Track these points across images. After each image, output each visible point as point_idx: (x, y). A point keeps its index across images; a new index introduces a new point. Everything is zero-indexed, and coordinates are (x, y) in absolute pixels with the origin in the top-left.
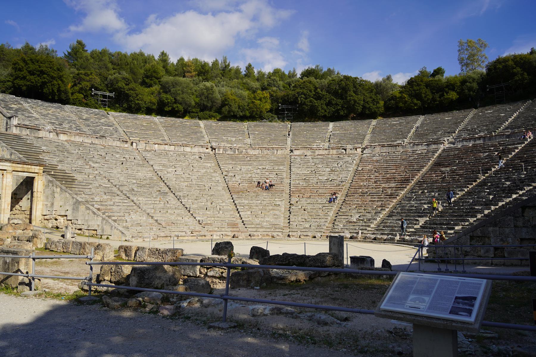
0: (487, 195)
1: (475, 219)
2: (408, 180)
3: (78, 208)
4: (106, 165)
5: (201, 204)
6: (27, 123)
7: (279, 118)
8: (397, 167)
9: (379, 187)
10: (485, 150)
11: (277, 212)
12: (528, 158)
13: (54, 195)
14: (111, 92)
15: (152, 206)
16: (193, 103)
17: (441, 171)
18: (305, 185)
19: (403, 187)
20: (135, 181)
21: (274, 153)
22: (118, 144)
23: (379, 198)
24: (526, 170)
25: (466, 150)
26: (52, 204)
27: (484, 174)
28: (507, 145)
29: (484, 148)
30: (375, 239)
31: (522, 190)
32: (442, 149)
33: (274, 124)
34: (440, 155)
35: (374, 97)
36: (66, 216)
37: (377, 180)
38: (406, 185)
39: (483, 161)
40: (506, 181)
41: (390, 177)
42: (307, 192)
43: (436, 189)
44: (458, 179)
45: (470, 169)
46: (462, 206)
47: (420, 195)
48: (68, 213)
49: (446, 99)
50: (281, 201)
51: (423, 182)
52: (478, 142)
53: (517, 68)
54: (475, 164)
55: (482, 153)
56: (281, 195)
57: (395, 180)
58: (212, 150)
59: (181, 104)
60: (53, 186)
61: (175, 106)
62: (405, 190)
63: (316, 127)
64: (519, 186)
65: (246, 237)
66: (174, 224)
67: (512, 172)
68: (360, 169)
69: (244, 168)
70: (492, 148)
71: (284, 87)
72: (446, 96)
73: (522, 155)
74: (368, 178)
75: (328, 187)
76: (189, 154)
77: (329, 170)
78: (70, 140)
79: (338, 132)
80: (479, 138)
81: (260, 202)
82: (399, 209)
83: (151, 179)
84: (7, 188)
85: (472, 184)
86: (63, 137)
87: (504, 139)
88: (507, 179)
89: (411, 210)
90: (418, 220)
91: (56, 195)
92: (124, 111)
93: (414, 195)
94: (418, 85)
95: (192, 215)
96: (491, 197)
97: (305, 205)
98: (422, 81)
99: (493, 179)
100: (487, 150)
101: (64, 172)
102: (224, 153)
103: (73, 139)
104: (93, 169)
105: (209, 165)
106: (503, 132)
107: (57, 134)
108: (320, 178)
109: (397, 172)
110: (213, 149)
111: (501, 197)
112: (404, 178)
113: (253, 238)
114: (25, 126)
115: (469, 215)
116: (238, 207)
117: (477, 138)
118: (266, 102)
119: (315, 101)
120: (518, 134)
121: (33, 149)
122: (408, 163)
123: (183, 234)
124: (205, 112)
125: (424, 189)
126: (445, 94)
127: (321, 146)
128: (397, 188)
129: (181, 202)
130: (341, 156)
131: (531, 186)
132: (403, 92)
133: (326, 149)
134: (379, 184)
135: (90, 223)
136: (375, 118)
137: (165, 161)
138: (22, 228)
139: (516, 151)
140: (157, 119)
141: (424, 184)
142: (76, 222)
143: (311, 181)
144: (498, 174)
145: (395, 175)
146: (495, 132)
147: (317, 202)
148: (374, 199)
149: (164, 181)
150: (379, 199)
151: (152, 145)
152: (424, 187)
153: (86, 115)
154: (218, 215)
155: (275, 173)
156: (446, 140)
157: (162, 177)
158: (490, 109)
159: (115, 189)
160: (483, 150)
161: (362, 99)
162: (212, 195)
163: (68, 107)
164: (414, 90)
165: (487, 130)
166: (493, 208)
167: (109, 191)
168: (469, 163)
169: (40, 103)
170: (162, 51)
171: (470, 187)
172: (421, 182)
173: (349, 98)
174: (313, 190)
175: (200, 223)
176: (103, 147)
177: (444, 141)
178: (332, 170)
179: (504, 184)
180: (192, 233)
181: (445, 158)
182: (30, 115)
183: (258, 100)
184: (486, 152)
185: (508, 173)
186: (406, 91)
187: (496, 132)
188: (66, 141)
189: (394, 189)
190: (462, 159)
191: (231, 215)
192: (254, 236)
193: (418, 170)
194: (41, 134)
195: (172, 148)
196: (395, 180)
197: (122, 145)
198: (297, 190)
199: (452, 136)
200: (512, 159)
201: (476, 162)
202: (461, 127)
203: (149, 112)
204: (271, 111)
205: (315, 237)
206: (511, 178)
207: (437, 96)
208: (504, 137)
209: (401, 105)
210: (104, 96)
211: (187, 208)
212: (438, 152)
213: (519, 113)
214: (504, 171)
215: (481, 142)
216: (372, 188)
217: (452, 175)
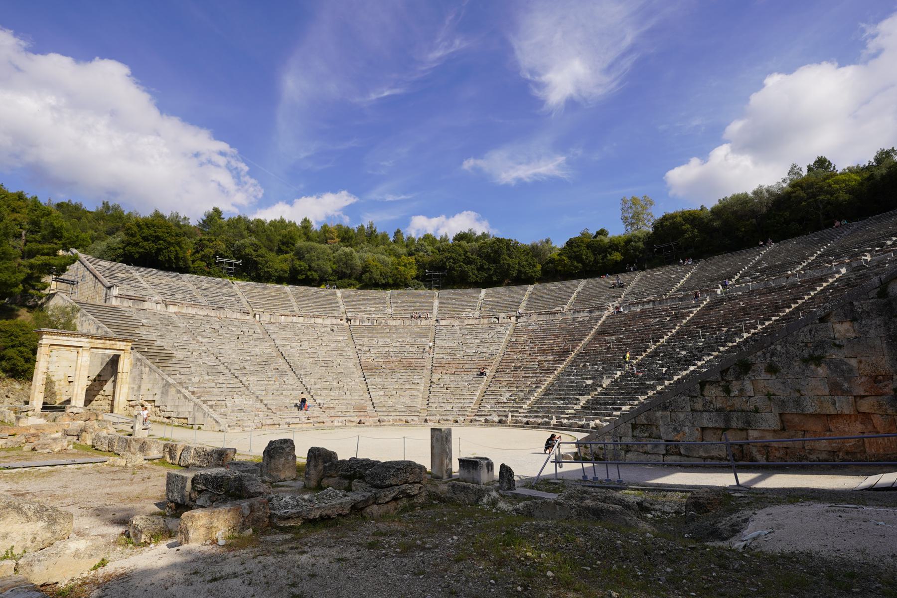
0: (659, 367)
1: (646, 397)
3: (167, 391)
4: (217, 340)
5: (325, 383)
6: (131, 293)
7: (426, 286)
8: (556, 336)
11: (414, 392)
12: (705, 323)
13: (141, 376)
14: (238, 259)
15: (263, 388)
16: (330, 270)
17: (605, 341)
18: (450, 359)
20: (249, 358)
22: (238, 316)
23: (533, 373)
24: (704, 336)
25: (634, 317)
26: (139, 387)
27: (655, 342)
28: (680, 309)
29: (654, 314)
30: (527, 423)
31: (700, 361)
33: (420, 291)
34: (604, 322)
35: (530, 260)
36: (154, 401)
39: (653, 328)
40: (680, 350)
43: (600, 361)
44: (625, 350)
45: (639, 337)
46: (631, 381)
48: (157, 398)
49: (609, 260)
50: (421, 378)
51: (585, 353)
52: (647, 306)
53: (686, 224)
56: (421, 371)
58: (347, 322)
59: (316, 271)
60: (141, 365)
61: (309, 273)
62: (565, 363)
63: (466, 294)
64: (696, 355)
65: (374, 423)
66: (287, 408)
67: (688, 340)
68: (513, 339)
69: (381, 341)
70: (663, 313)
72: (609, 257)
73: (698, 320)
75: (476, 362)
76: (320, 326)
77: (479, 341)
78: (180, 312)
79: (491, 299)
80: (648, 302)
81: (395, 380)
82: (557, 385)
83: (270, 355)
84: (82, 369)
85: (641, 355)
86: (172, 309)
87: (677, 303)
88: (683, 348)
89: (571, 387)
90: (578, 399)
91: (144, 376)
92: (252, 279)
93: (575, 369)
94: (578, 246)
95: (312, 396)
96: (664, 369)
98: (582, 242)
99: (667, 349)
101: (162, 348)
102: (361, 324)
103: (184, 310)
104: (200, 344)
105: (341, 338)
107: (166, 306)
108: (468, 351)
110: (348, 320)
111: (676, 369)
113: (382, 423)
114: (127, 297)
115: (638, 392)
116: (369, 387)
117: (646, 302)
118: (411, 268)
119: (465, 266)
121: (130, 323)
123: (297, 420)
124: (343, 280)
125: (586, 361)
126: (608, 255)
127: (471, 315)
129: (302, 382)
130: (493, 326)
132: (562, 255)
133: (476, 319)
134: (534, 357)
135: (180, 410)
136: (532, 284)
137: (289, 335)
138: (84, 419)
139: (691, 315)
140: (288, 288)
141: (586, 355)
142: (164, 408)
143: (457, 355)
144: (672, 342)
146: (665, 295)
148: (528, 375)
149: (284, 357)
150: (534, 375)
151: (277, 317)
152: (586, 360)
153: (207, 285)
154: (344, 397)
155: (416, 346)
157: (283, 353)
158: (659, 271)
159: (222, 368)
161: (517, 262)
162: (340, 373)
163: (186, 277)
164: (574, 252)
165: (657, 293)
166: (667, 383)
167: (214, 370)
168: (637, 330)
169: (154, 272)
170: (304, 218)
171: (640, 358)
172: (582, 353)
173: (502, 262)
175: (321, 406)
176: (218, 320)
178: (482, 342)
179: (678, 354)
180: (308, 419)
182: (138, 284)
183: (403, 266)
184: (657, 317)
185: (682, 341)
186: (565, 253)
187: (666, 295)
188: (175, 313)
190: (630, 326)
191: (360, 396)
192: (384, 421)
194: (146, 305)
195: (301, 319)
196: (553, 352)
197: (242, 318)
198: (440, 365)
200: (687, 325)
201: (646, 329)
203: (280, 280)
204: (417, 277)
205: (457, 422)
206: (687, 346)
207: (600, 257)
209: (560, 268)
210: (231, 264)
211: (307, 389)
212: (602, 319)
213: (692, 273)
214: (678, 338)
215: (651, 306)
216: (527, 361)
217: (618, 345)
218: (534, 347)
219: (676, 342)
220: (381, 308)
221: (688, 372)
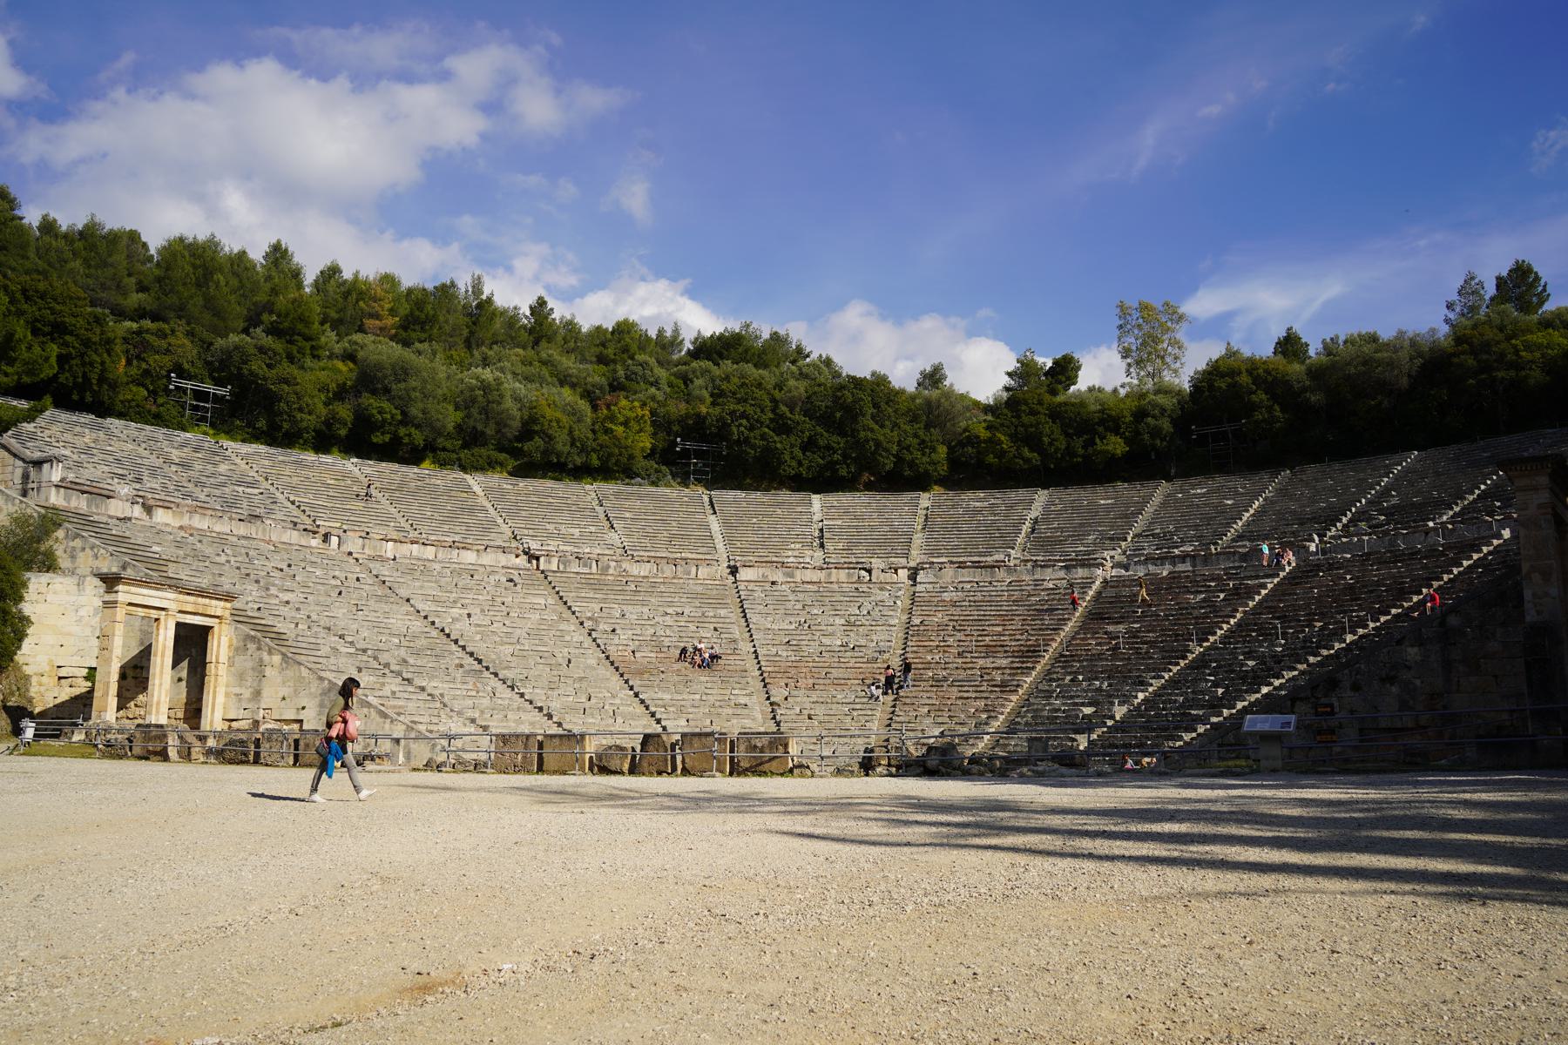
0: (1211, 687)
2: (1035, 651)
9: (970, 665)
10: (1198, 586)
17: (1106, 633)
18: (793, 659)
19: (1027, 668)
21: (689, 573)
23: (976, 691)
24: (1284, 635)
25: (1157, 586)
27: (1201, 640)
28: (1243, 579)
29: (1195, 584)
34: (1099, 593)
37: (964, 648)
38: (1032, 662)
39: (1196, 613)
40: (1246, 659)
41: (994, 643)
42: (802, 675)
44: (1146, 653)
45: (1170, 630)
47: (1069, 686)
51: (1072, 656)
52: (1181, 567)
54: (1179, 619)
55: (1192, 593)
57: (1006, 652)
62: (1034, 673)
67: (1259, 641)
68: (917, 621)
70: (1213, 584)
71: (670, 385)
74: (942, 644)
75: (851, 665)
77: (843, 621)
80: (1183, 558)
85: (1178, 664)
87: (1237, 564)
88: (1249, 655)
93: (1057, 686)
97: (808, 706)
100: (1202, 586)
106: (1233, 547)
108: (826, 641)
109: (1007, 633)
111: (1241, 690)
117: (1178, 556)
122: (1029, 611)
128: (1014, 668)
131: (1295, 669)
139: (1264, 592)
141: (1074, 661)
144: (1230, 643)
145: (1002, 638)
146: (1216, 544)
147: (834, 700)
148: (966, 695)
150: (978, 695)
156: (1108, 558)
158: (1199, 485)
160: (1193, 586)
165: (1199, 538)
168: (1166, 615)
171: (1175, 669)
172: (1066, 656)
174: (817, 670)
177: (1105, 559)
178: (849, 623)
179: (1242, 665)
181: (1111, 603)
184: (1201, 592)
185: (1249, 642)
193: (1054, 629)
196: (1006, 652)
199: (1120, 547)
201: (1182, 614)
202: (1139, 525)
206: (1256, 652)
208: (1237, 557)
212: (1094, 587)
213: (1265, 499)
214: (1242, 636)
216: (957, 668)
217: (1133, 643)
218: (963, 638)
219: (1238, 642)
221: (1258, 696)
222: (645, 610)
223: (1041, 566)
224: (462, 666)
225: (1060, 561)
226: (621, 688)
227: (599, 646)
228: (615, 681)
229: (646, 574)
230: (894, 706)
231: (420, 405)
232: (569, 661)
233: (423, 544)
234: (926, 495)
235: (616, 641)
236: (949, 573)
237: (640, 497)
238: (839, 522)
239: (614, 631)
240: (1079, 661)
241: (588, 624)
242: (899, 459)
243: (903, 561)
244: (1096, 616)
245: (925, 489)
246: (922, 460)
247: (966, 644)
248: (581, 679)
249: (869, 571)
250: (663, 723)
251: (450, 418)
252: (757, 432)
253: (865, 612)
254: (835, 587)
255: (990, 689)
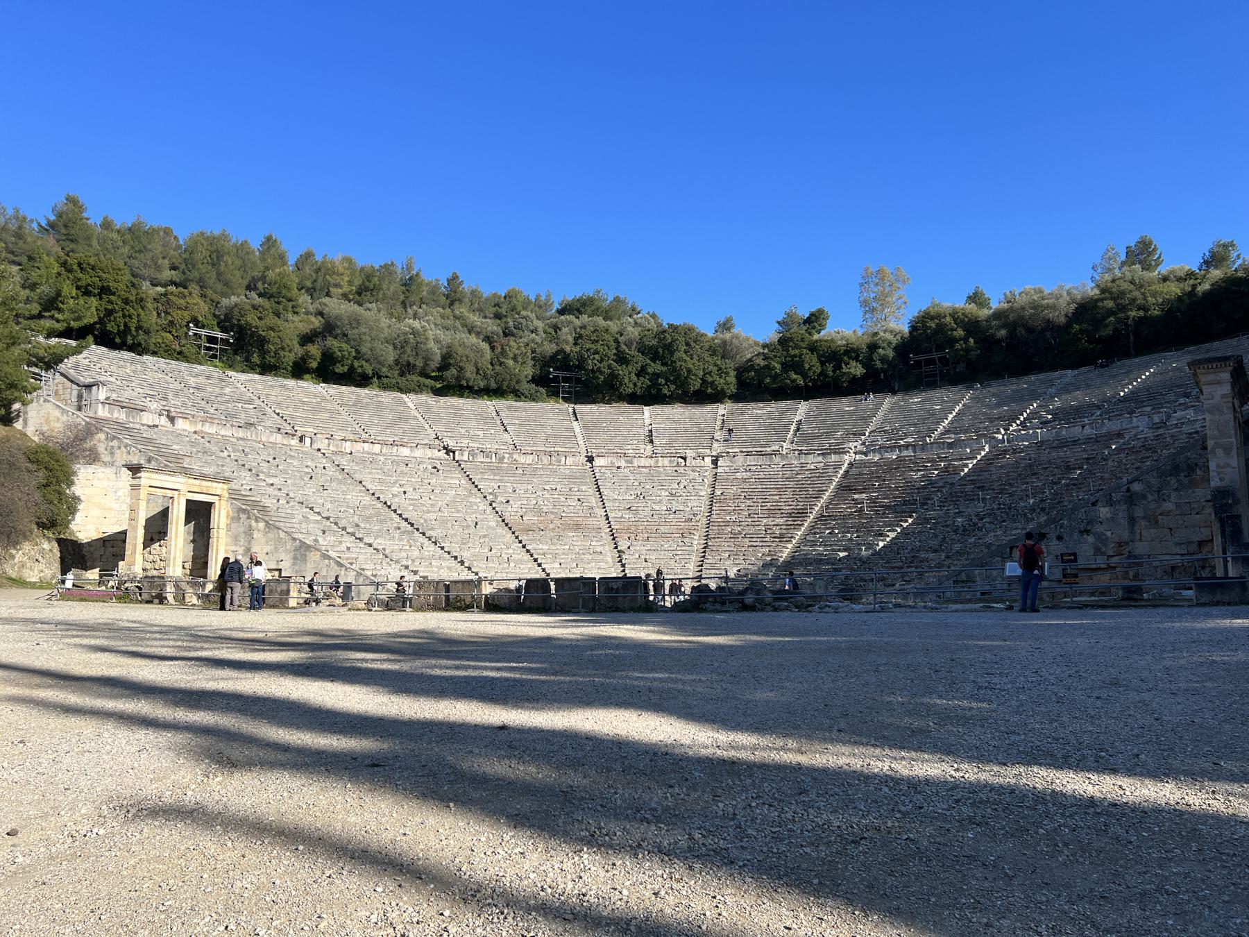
8: (781, 490)
17: (853, 500)
21: (560, 461)
28: (951, 460)
32: (848, 462)
34: (847, 472)
39: (917, 485)
42: (640, 531)
47: (829, 537)
52: (905, 453)
55: (914, 471)
57: (782, 513)
71: (545, 332)
74: (737, 508)
75: (674, 524)
80: (907, 447)
87: (946, 451)
93: (820, 537)
97: (644, 552)
106: (942, 439)
109: (782, 500)
112: (796, 509)
120: (966, 442)
134: (756, 520)
144: (944, 506)
146: (930, 437)
148: (755, 544)
150: (764, 544)
152: (831, 525)
156: (853, 447)
172: (825, 516)
174: (650, 527)
181: (856, 479)
187: (931, 437)
189: (784, 527)
190: (884, 480)
196: (782, 513)
199: (861, 440)
202: (874, 423)
218: (752, 504)
220: (493, 431)
222: (530, 487)
223: (805, 454)
224: (399, 528)
225: (818, 450)
226: (514, 542)
227: (497, 512)
228: (509, 537)
229: (530, 462)
230: (704, 552)
231: (368, 345)
232: (476, 524)
233: (372, 443)
234: (723, 406)
235: (510, 509)
236: (740, 459)
237: (525, 409)
238: (663, 425)
239: (508, 502)
240: (835, 520)
241: (490, 498)
242: (704, 381)
243: (708, 451)
244: (846, 488)
245: (722, 403)
246: (720, 382)
247: (754, 508)
248: (485, 536)
249: (685, 459)
250: (543, 566)
251: (390, 355)
252: (605, 363)
253: (682, 487)
254: (662, 469)
255: (772, 540)
